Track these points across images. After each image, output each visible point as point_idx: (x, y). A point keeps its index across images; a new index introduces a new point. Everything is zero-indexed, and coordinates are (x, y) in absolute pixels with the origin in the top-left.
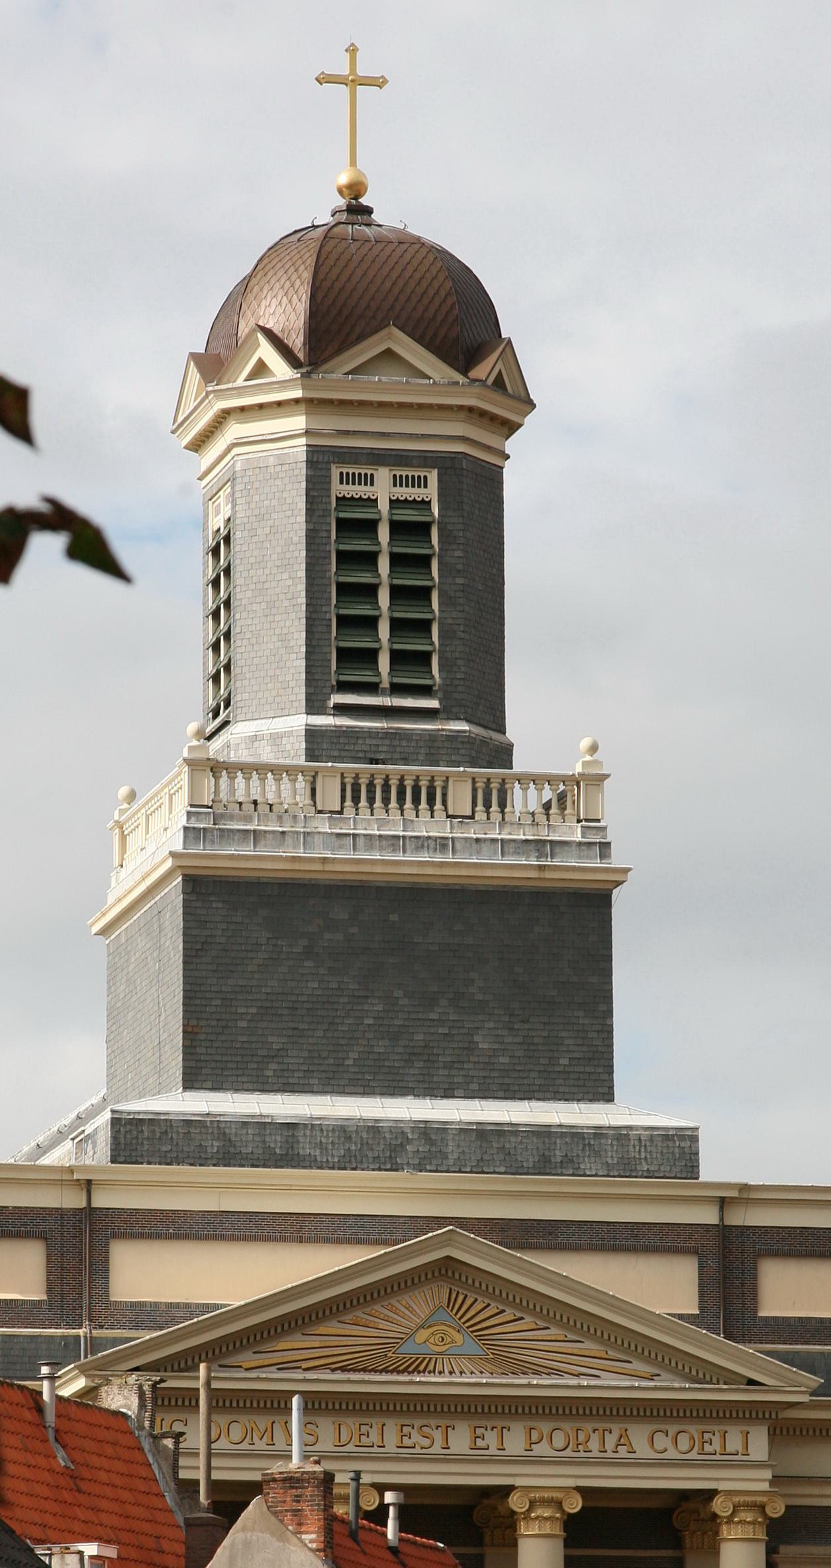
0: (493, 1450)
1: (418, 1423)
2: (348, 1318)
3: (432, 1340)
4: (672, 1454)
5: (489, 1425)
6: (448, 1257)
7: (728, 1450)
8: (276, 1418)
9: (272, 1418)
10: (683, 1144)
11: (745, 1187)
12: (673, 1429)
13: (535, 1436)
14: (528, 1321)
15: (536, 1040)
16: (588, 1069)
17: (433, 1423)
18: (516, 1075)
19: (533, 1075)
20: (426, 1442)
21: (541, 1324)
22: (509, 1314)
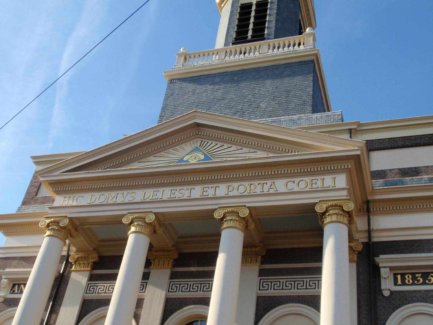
0: (210, 196)
1: (178, 188)
2: (157, 155)
3: (191, 159)
4: (296, 189)
5: (210, 186)
6: (196, 123)
7: (325, 186)
8: (119, 192)
9: (118, 192)
10: (334, 117)
11: (359, 125)
12: (297, 180)
13: (231, 189)
14: (234, 148)
15: (283, 102)
16: (302, 107)
17: (185, 188)
18: (275, 112)
19: (280, 111)
20: (181, 195)
21: (239, 148)
22: (226, 146)
